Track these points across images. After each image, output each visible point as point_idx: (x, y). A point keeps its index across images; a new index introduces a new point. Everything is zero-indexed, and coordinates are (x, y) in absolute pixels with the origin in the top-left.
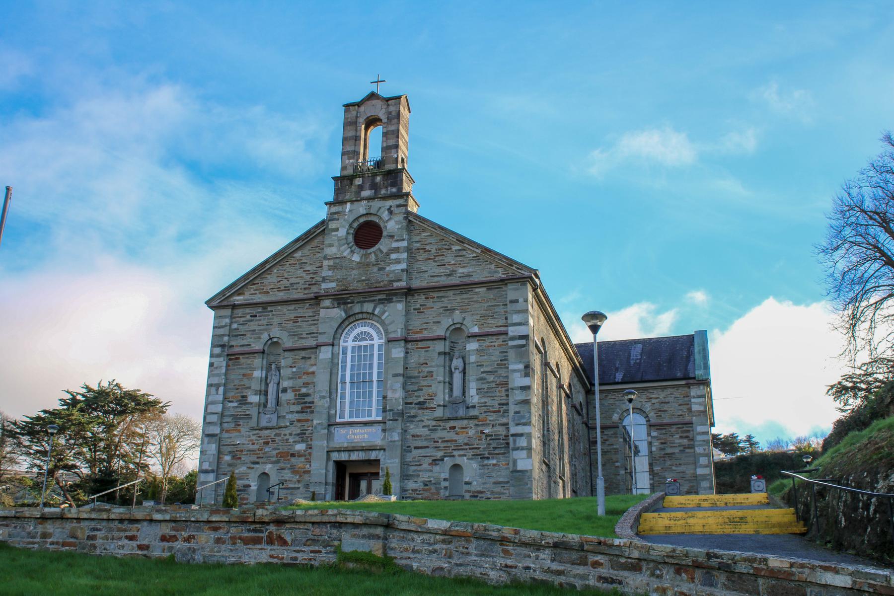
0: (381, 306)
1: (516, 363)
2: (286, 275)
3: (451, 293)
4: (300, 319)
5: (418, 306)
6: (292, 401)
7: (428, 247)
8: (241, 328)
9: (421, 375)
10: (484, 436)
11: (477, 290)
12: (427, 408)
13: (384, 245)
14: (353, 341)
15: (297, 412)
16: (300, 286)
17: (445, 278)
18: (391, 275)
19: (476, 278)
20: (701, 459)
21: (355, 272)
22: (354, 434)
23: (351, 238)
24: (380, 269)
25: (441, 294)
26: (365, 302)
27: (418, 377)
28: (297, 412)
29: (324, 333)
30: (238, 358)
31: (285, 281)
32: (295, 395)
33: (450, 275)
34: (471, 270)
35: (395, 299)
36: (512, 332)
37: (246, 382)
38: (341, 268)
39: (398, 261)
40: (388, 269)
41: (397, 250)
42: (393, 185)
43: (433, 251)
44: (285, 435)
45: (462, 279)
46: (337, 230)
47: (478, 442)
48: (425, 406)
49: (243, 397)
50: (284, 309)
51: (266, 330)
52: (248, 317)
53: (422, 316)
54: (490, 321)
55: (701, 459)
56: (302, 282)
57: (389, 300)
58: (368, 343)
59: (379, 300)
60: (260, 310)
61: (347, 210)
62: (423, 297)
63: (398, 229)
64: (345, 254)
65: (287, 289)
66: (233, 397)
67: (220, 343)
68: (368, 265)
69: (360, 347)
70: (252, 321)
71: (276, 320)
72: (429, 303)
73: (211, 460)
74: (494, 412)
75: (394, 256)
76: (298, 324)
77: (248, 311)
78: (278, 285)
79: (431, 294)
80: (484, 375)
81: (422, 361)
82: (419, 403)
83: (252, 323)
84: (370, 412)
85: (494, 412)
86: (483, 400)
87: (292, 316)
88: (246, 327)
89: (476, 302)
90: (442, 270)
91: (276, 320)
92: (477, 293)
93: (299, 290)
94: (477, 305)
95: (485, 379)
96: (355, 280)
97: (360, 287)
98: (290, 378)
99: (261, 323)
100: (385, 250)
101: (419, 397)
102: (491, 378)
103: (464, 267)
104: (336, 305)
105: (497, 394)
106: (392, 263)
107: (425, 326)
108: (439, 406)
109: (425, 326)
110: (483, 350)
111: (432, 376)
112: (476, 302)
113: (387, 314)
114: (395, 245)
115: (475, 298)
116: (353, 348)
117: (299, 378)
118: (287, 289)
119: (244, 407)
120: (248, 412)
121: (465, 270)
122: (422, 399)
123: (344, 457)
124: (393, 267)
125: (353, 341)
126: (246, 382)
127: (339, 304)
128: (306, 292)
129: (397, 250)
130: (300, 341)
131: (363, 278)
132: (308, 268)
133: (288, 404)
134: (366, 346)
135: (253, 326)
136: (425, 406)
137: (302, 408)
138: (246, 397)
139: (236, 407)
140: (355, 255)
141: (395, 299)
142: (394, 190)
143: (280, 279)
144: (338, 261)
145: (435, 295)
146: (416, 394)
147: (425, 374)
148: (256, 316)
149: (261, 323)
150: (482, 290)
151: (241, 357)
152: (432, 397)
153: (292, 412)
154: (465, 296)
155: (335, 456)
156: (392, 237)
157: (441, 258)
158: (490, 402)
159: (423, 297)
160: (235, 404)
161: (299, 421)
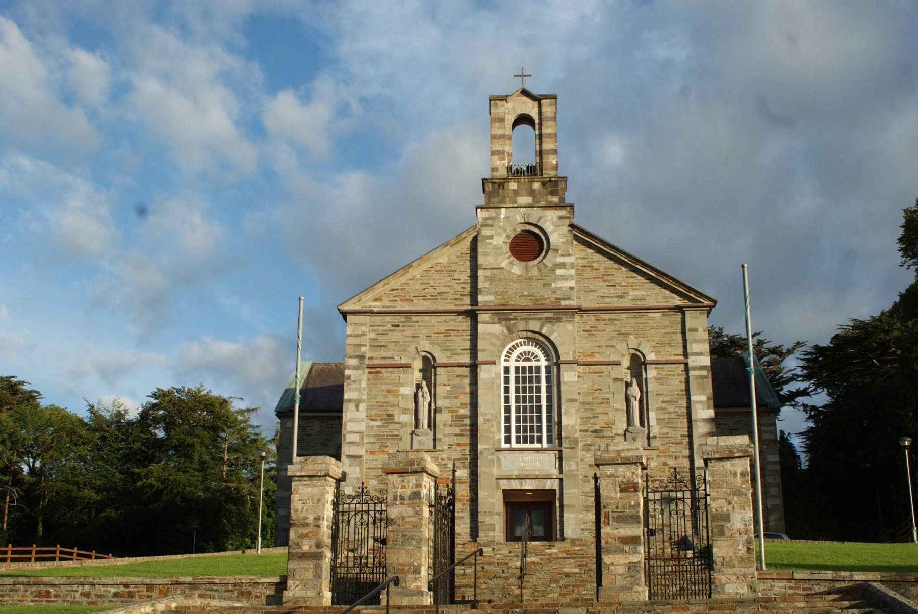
0: (549, 325)
1: (698, 394)
2: (432, 283)
3: (624, 316)
4: (452, 333)
5: (588, 328)
6: (449, 423)
7: (595, 265)
8: (381, 338)
9: (596, 401)
10: (666, 468)
11: (651, 315)
12: (604, 437)
13: (550, 259)
14: (516, 360)
15: (456, 435)
16: (450, 296)
17: (615, 300)
18: (558, 292)
19: (650, 303)
20: (771, 489)
21: (516, 286)
22: (525, 462)
23: (507, 248)
24: (545, 285)
25: (613, 316)
26: (530, 319)
27: (592, 403)
28: (456, 435)
29: (485, 350)
30: (380, 372)
31: (432, 290)
32: (453, 416)
33: (621, 297)
34: (644, 293)
35: (564, 318)
36: (693, 361)
37: (391, 399)
38: (500, 280)
39: (565, 278)
40: (553, 285)
41: (562, 266)
42: (553, 193)
43: (602, 270)
44: (443, 459)
45: (635, 302)
46: (491, 237)
47: (661, 474)
48: (601, 435)
49: (388, 415)
50: (434, 319)
51: (413, 342)
52: (389, 327)
53: (593, 338)
54: (668, 348)
55: (771, 489)
56: (452, 291)
57: (559, 320)
58: (534, 364)
59: (547, 318)
60: (403, 319)
61: (502, 216)
62: (593, 318)
63: (563, 243)
64: (503, 265)
65: (434, 298)
66: (375, 415)
67: (358, 354)
68: (531, 279)
69: (524, 368)
70: (394, 331)
71: (424, 332)
72: (601, 325)
73: (355, 484)
74: (677, 443)
75: (559, 272)
76: (450, 338)
77: (388, 318)
78: (423, 293)
79: (602, 315)
80: (664, 405)
81: (596, 387)
82: (595, 431)
83: (395, 334)
84: (540, 440)
85: (677, 443)
86: (665, 431)
87: (443, 329)
88: (386, 337)
89: (652, 328)
90: (612, 290)
91: (424, 332)
92: (652, 318)
93: (449, 301)
94: (653, 331)
95: (665, 409)
96: (518, 296)
97: (524, 303)
98: (445, 398)
99: (404, 334)
100: (550, 265)
101: (595, 424)
102: (671, 408)
103: (635, 289)
104: (496, 321)
105: (679, 425)
106: (558, 279)
107: (596, 350)
108: (617, 435)
109: (596, 350)
110: (661, 379)
111: (608, 403)
112: (652, 328)
113: (556, 334)
114: (560, 260)
115: (651, 323)
116: (517, 368)
117: (456, 397)
118: (434, 298)
119: (391, 427)
120: (396, 433)
121: (636, 293)
122: (597, 427)
123: (515, 485)
124: (560, 284)
125: (516, 360)
126: (391, 399)
127: (499, 319)
128: (459, 303)
129: (562, 266)
130: (455, 357)
131: (526, 293)
132: (456, 276)
133: (444, 425)
134: (531, 368)
135: (395, 336)
136: (601, 435)
137: (461, 431)
138: (392, 415)
139: (382, 426)
140: (515, 267)
141: (564, 318)
142: (555, 199)
143: (424, 286)
144: (495, 272)
145: (607, 316)
146: (592, 421)
147: (600, 401)
148: (398, 326)
149: (404, 334)
150: (657, 315)
151: (383, 370)
152: (610, 425)
153: (449, 435)
154: (639, 320)
155: (505, 484)
156: (556, 251)
157: (610, 278)
158: (671, 433)
159: (593, 318)
160: (379, 423)
161: (458, 445)
